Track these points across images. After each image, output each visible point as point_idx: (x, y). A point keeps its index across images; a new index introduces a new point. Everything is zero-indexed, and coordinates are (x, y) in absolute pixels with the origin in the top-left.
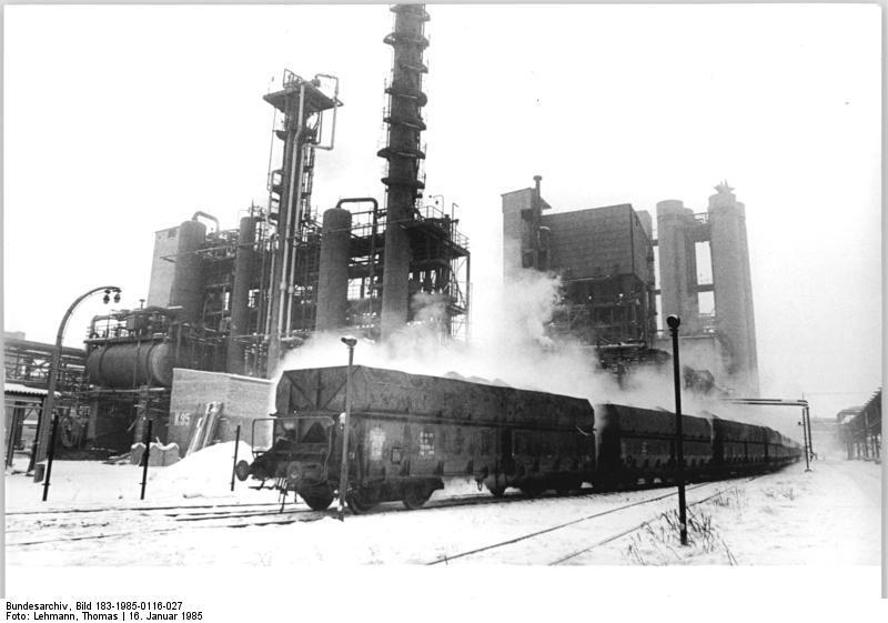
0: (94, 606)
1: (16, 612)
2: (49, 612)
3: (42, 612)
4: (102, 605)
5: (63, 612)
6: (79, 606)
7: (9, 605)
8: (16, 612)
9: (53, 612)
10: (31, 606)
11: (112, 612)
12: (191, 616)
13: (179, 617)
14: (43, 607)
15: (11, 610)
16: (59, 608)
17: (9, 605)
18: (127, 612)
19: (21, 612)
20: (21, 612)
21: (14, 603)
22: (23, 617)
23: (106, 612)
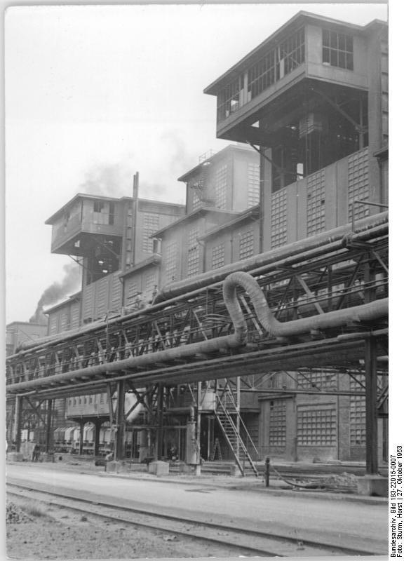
0: (393, 502)
1: (397, 551)
3: (397, 534)
4: (392, 496)
6: (393, 511)
7: (393, 556)
8: (397, 551)
9: (397, 528)
10: (394, 541)
13: (400, 460)
14: (394, 534)
15: (396, 554)
16: (394, 523)
19: (397, 548)
20: (397, 548)
21: (390, 552)
22: (401, 546)
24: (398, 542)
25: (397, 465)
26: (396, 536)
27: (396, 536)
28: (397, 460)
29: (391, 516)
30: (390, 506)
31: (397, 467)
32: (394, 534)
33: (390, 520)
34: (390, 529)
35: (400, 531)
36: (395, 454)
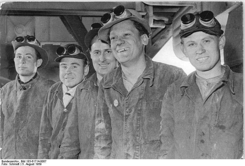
1: (4, 163)
2: (14, 163)
3: (11, 163)
8: (4, 163)
10: (9, 161)
14: (12, 162)
15: (3, 162)
16: (16, 162)
19: (6, 163)
20: (6, 163)
22: (6, 164)
24: (8, 163)
25: (33, 163)
27: (11, 163)
29: (20, 160)
30: (24, 160)
31: (31, 163)
32: (12, 162)
33: (18, 160)
34: (14, 160)
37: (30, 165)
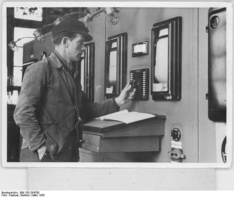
0: (25, 193)
1: (4, 194)
4: (27, 192)
5: (17, 194)
6: (21, 192)
7: (2, 192)
8: (4, 194)
10: (8, 193)
11: (29, 194)
12: (41, 195)
14: (11, 193)
15: (3, 194)
16: (16, 193)
17: (2, 192)
18: (32, 194)
19: (6, 194)
20: (6, 194)
21: (4, 191)
22: (6, 195)
23: (27, 194)
24: (8, 194)
26: (10, 194)
27: (10, 194)
28: (38, 194)
32: (11, 193)
35: (13, 196)
36: (40, 193)
37: (35, 195)
